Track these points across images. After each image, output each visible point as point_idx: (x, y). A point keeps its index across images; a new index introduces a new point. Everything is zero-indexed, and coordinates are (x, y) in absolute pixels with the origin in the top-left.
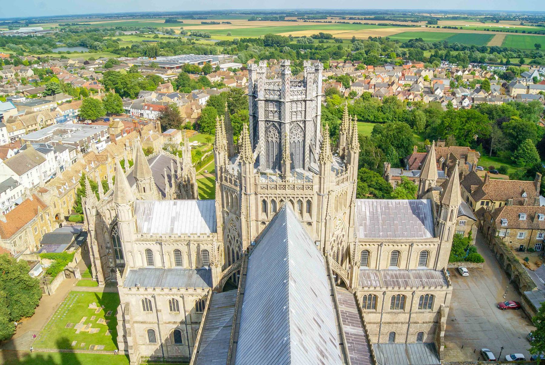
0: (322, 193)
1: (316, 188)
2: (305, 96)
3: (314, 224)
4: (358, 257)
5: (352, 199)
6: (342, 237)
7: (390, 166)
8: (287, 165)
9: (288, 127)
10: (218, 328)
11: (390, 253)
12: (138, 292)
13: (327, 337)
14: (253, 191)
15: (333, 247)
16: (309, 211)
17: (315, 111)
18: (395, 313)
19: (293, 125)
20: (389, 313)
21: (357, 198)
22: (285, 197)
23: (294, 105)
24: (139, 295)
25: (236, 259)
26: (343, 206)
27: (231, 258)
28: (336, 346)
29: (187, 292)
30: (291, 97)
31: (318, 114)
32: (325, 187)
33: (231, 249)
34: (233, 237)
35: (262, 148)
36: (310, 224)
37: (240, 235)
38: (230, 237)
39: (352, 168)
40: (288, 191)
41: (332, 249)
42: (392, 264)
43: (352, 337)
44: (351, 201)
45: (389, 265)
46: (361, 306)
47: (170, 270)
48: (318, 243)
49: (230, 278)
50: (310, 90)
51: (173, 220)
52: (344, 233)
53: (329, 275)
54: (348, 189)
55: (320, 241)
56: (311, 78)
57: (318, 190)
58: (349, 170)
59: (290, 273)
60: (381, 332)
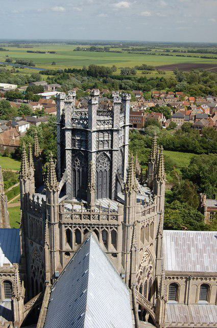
0: (127, 224)
1: (121, 218)
2: (111, 126)
3: (120, 255)
4: (165, 291)
5: (159, 230)
6: (149, 269)
7: (205, 197)
8: (92, 194)
9: (94, 156)
11: (199, 287)
14: (57, 221)
15: (139, 279)
16: (115, 243)
17: (123, 141)
19: (99, 154)
21: (164, 229)
22: (89, 227)
23: (101, 134)
26: (150, 237)
31: (126, 144)
32: (131, 217)
33: (35, 281)
34: (36, 267)
35: (69, 177)
36: (115, 255)
37: (44, 266)
39: (158, 199)
40: (93, 221)
41: (138, 282)
44: (158, 233)
45: (198, 298)
48: (123, 276)
53: (134, 309)
54: (155, 219)
57: (123, 221)
58: (156, 199)
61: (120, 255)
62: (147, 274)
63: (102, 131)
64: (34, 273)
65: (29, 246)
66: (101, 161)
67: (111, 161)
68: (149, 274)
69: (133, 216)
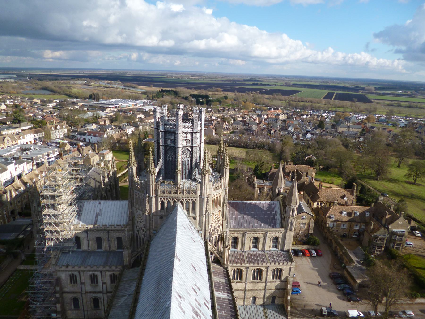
1: (198, 193)
2: (191, 130)
3: (198, 218)
4: (230, 242)
6: (218, 228)
7: (256, 178)
9: (180, 150)
10: (125, 296)
11: (252, 239)
12: (67, 269)
13: (202, 302)
16: (194, 209)
18: (256, 283)
20: (251, 282)
22: (177, 199)
24: (67, 271)
25: (142, 243)
26: (218, 205)
27: (139, 243)
28: (208, 308)
29: (104, 269)
30: (183, 130)
32: (205, 192)
33: (139, 236)
38: (138, 228)
42: (98, 248)
43: (223, 301)
45: (251, 247)
46: (231, 277)
47: (93, 252)
49: (138, 256)
50: (196, 125)
51: (97, 215)
52: (220, 225)
53: (207, 255)
55: (202, 230)
56: (196, 117)
58: (222, 180)
59: (176, 253)
60: (246, 297)
61: (198, 218)
62: (216, 231)
63: (186, 133)
64: (138, 231)
65: (135, 212)
66: (185, 154)
67: (191, 154)
68: (218, 231)
69: (207, 191)
